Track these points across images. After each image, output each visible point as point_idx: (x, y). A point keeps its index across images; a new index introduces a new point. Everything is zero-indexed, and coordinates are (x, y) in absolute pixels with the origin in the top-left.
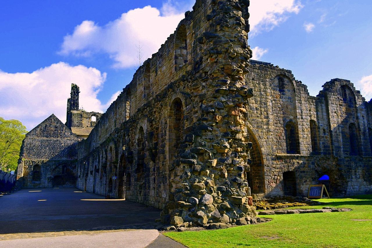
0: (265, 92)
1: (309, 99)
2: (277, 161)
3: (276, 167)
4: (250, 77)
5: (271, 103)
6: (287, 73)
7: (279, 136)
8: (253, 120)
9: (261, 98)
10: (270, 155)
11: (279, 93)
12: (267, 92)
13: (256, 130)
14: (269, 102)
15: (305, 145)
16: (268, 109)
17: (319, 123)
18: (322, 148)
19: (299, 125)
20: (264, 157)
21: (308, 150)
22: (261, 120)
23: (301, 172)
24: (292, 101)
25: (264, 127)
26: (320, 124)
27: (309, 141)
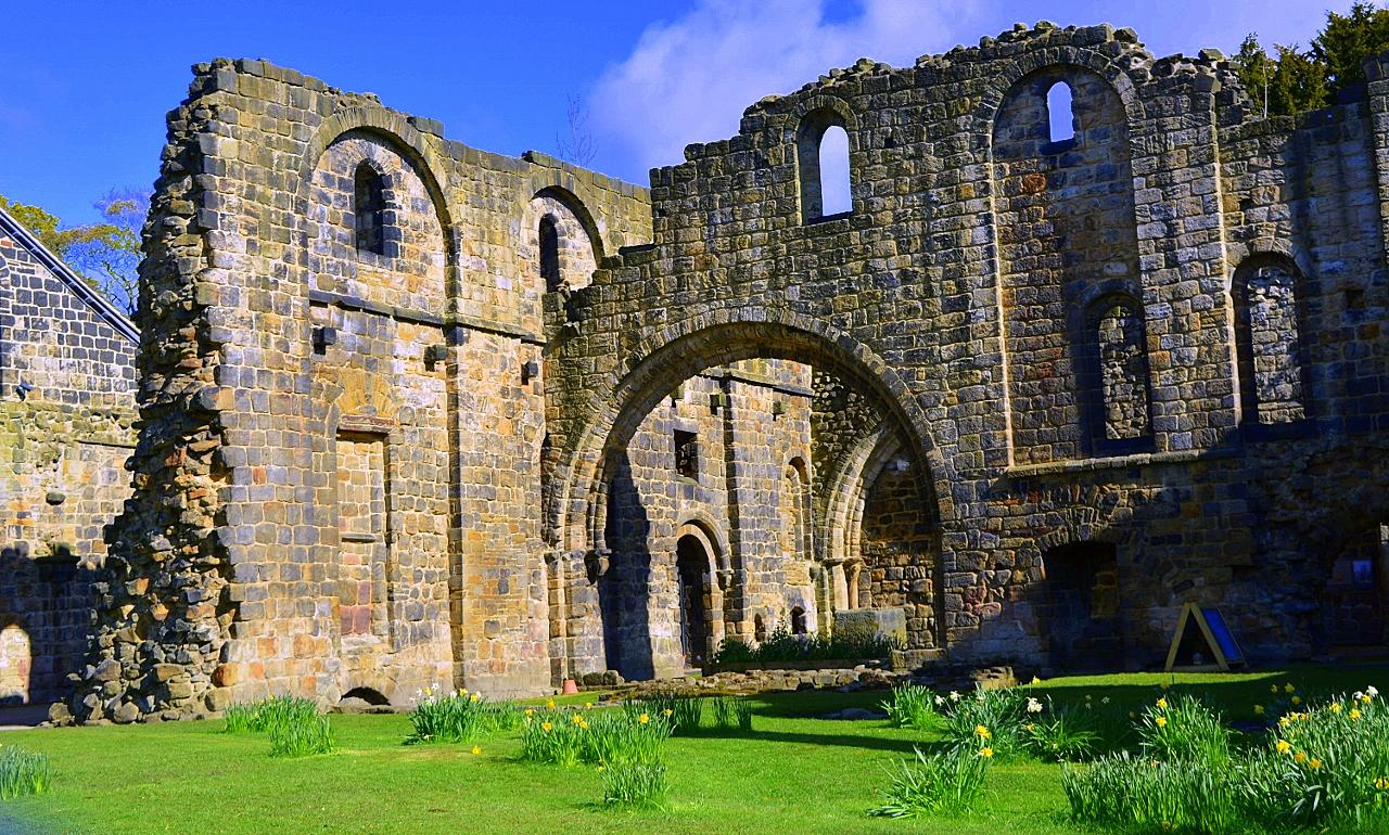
0: (948, 182)
1: (1241, 140)
2: (1009, 502)
3: (1003, 528)
4: (872, 139)
5: (981, 232)
6: (1077, 46)
7: (1038, 378)
8: (889, 330)
9: (927, 219)
10: (975, 478)
11: (1042, 166)
12: (962, 182)
13: (900, 372)
14: (973, 227)
15: (1187, 400)
16: (966, 262)
17: (1315, 258)
18: (1333, 400)
19: (1154, 301)
20: (939, 489)
21: (1211, 425)
22: (925, 324)
23: (1156, 541)
24: (1123, 184)
25: (940, 351)
26: (1324, 266)
27: (1220, 376)
